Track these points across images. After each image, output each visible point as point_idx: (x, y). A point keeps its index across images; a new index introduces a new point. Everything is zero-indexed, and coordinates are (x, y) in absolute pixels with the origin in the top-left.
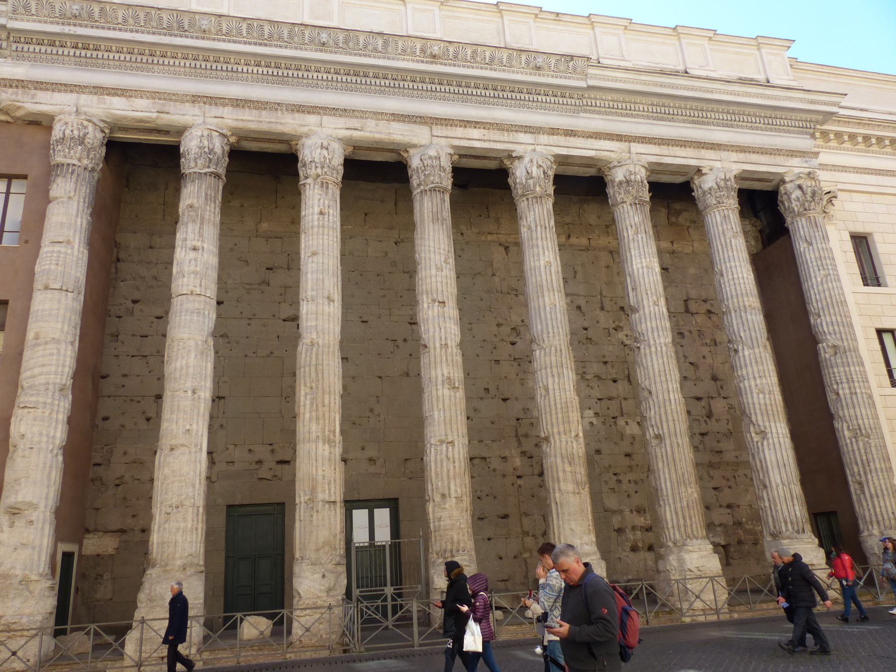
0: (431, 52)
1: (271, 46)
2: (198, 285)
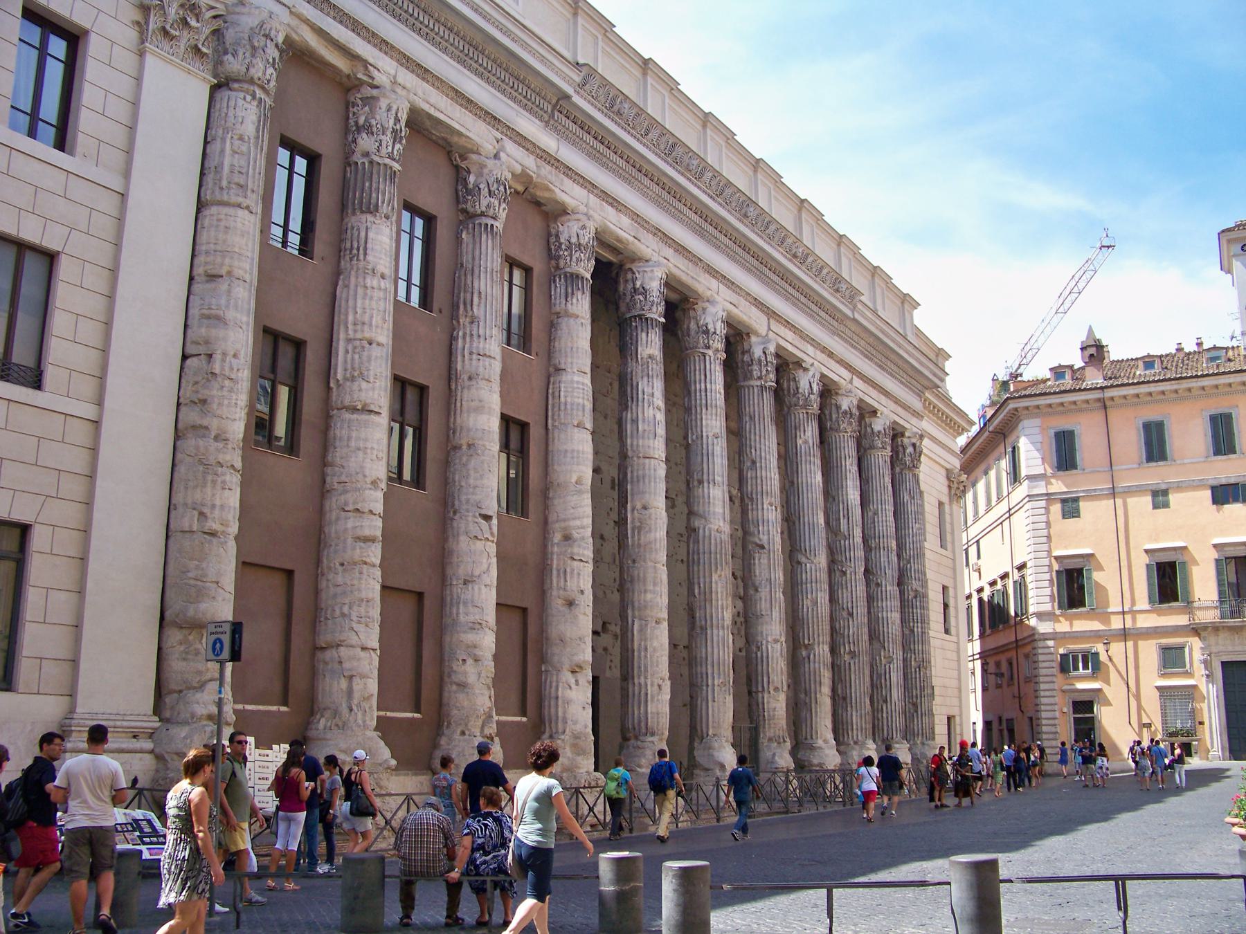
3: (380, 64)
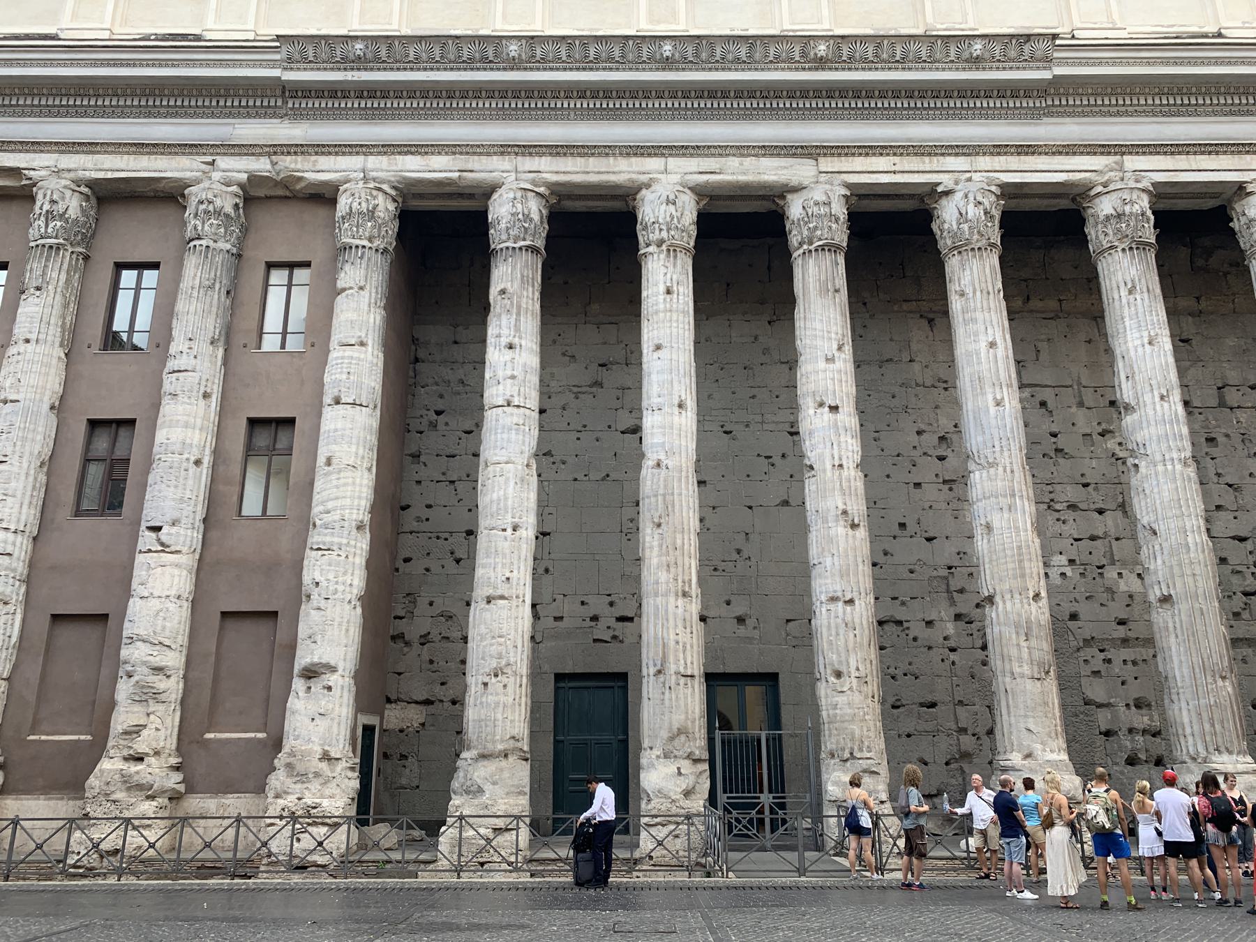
0: (816, 54)
1: (597, 69)
2: (515, 394)
3: (35, 164)
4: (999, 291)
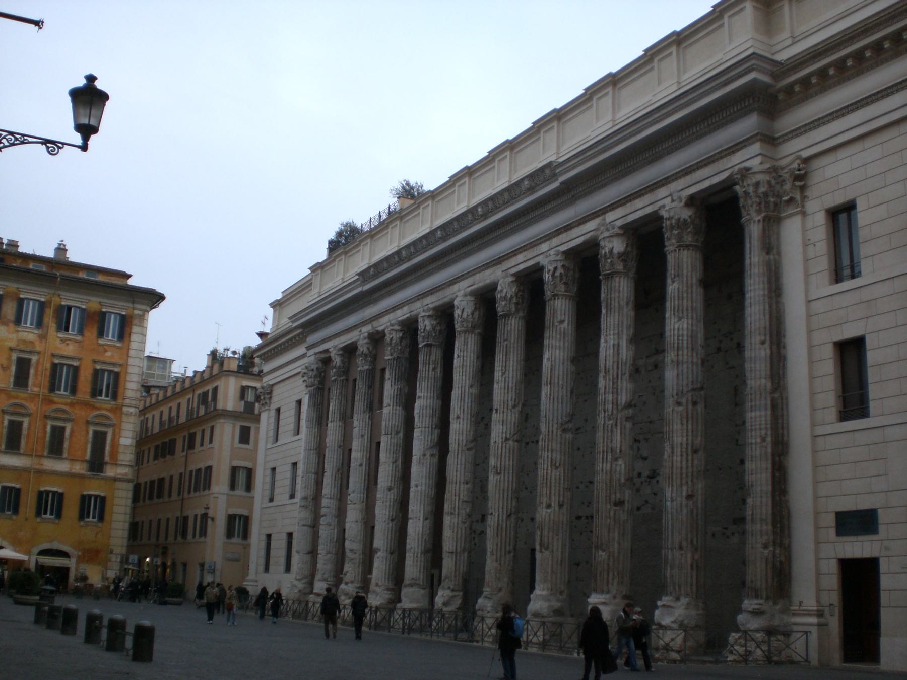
4: (562, 322)
